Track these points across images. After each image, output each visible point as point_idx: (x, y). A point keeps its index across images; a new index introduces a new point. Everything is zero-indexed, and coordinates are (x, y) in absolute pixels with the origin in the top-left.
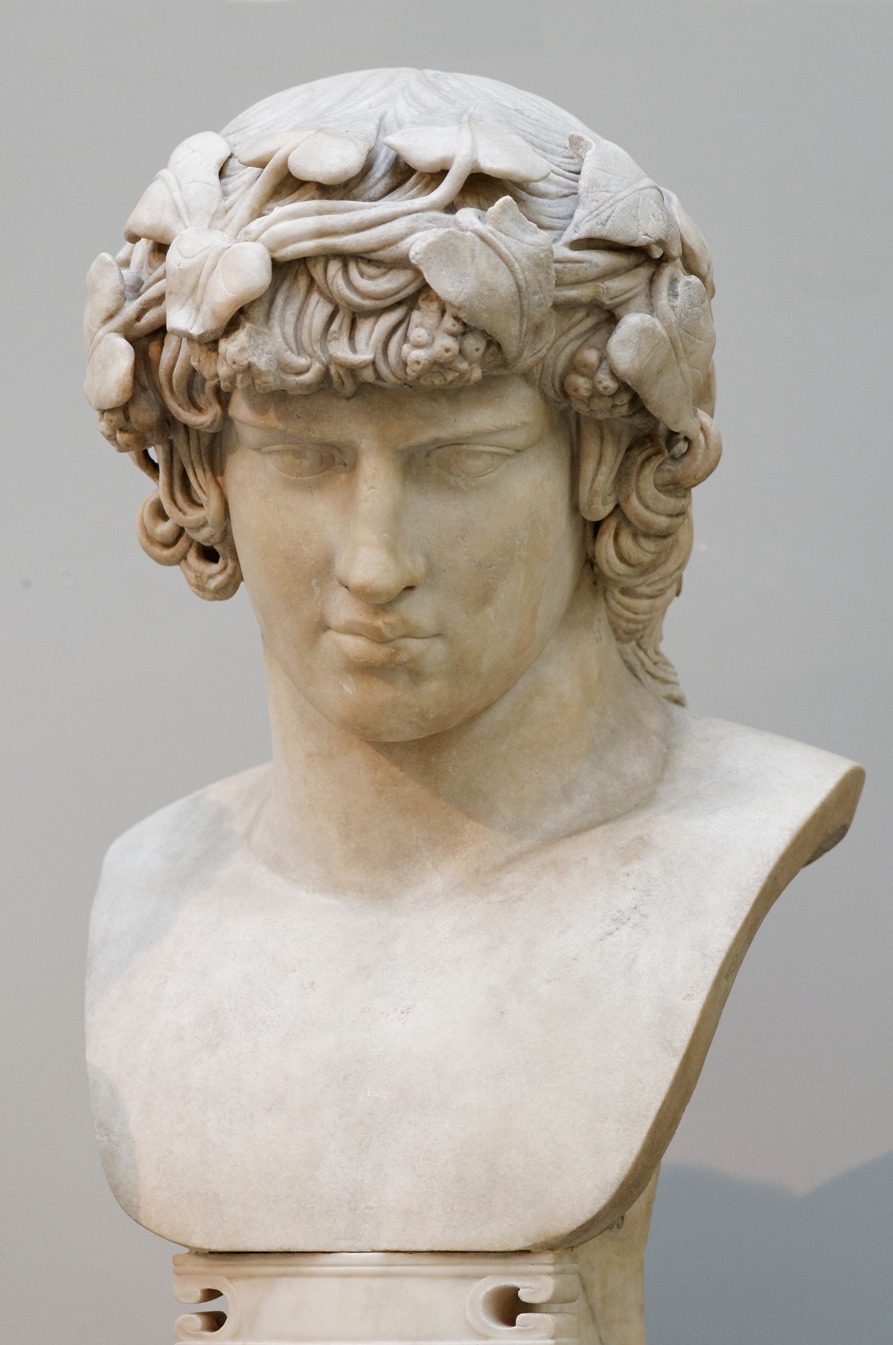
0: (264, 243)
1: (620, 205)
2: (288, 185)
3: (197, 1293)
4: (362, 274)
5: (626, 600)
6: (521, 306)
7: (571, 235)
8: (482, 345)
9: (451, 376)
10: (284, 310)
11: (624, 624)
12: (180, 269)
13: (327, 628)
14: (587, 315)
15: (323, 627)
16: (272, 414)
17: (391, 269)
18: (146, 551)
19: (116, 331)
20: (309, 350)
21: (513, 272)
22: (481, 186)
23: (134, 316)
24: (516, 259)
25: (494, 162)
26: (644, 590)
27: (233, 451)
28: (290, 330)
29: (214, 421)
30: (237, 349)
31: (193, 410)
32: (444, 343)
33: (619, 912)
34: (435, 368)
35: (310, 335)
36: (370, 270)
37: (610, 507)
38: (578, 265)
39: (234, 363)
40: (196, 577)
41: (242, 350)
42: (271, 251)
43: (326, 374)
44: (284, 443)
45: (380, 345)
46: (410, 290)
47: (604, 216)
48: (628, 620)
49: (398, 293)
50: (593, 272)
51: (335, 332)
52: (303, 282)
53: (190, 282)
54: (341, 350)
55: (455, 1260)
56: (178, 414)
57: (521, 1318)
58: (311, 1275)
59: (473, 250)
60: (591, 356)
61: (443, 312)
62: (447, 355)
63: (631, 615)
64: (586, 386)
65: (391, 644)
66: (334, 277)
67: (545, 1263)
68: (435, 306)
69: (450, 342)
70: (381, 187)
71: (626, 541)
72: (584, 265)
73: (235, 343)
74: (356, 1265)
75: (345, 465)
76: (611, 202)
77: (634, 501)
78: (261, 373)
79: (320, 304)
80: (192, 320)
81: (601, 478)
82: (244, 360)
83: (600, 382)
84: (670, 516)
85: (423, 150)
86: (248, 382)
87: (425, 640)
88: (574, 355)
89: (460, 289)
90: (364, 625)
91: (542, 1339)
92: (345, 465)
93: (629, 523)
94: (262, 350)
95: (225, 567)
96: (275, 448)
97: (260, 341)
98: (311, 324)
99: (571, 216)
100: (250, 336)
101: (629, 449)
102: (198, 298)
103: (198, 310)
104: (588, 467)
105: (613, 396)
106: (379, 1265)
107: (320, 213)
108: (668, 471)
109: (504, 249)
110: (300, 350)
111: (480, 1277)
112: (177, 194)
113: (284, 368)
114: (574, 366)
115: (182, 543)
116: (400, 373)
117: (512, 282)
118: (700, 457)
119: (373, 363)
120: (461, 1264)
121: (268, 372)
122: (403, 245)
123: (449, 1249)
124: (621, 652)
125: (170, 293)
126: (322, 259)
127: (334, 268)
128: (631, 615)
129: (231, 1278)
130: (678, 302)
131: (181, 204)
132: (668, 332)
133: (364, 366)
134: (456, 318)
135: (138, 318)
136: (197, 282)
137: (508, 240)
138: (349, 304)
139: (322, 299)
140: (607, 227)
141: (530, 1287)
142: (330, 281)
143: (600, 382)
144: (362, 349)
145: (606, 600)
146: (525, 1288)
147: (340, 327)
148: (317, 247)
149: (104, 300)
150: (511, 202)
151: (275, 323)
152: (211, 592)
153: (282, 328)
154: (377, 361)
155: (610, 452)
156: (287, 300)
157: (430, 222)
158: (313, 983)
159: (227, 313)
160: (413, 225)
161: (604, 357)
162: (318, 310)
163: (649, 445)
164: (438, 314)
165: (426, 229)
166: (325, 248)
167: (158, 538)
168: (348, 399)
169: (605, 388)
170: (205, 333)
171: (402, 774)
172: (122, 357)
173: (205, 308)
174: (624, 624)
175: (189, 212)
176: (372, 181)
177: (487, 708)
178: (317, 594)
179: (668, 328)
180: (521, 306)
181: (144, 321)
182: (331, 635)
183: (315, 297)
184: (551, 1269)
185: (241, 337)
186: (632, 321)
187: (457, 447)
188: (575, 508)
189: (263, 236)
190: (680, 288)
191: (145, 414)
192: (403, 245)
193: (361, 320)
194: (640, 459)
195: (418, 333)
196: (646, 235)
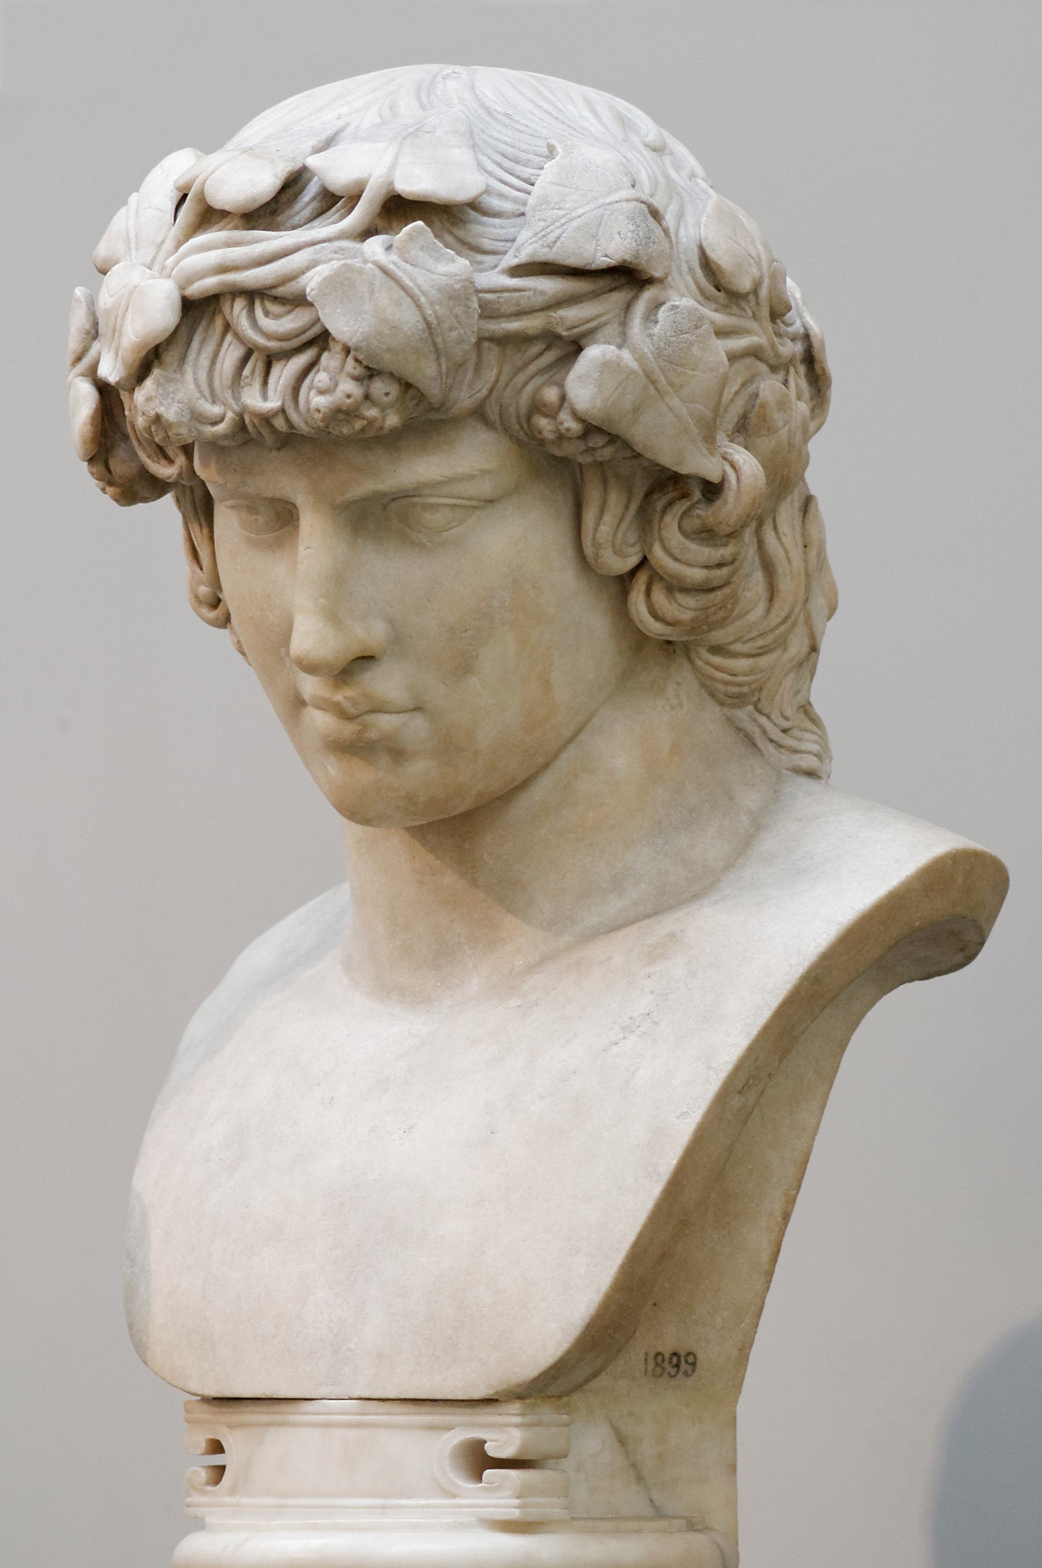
1: (575, 224)
3: (201, 1441)
4: (267, 314)
5: (717, 660)
7: (511, 260)
8: (394, 390)
10: (199, 352)
11: (721, 687)
14: (548, 348)
15: (299, 703)
17: (297, 306)
21: (419, 307)
22: (397, 209)
24: (423, 293)
25: (417, 182)
26: (738, 647)
28: (203, 376)
31: (163, 462)
32: (348, 387)
36: (274, 308)
37: (633, 561)
38: (517, 294)
41: (149, 399)
42: (182, 288)
43: (240, 426)
45: (289, 391)
47: (552, 237)
48: (726, 683)
49: (304, 332)
50: (538, 301)
52: (219, 324)
55: (424, 1409)
58: (296, 1425)
60: (551, 394)
62: (349, 401)
63: (727, 677)
64: (549, 428)
65: (358, 720)
66: (238, 316)
67: (512, 1413)
70: (307, 212)
71: (659, 597)
72: (527, 293)
76: (563, 221)
78: (170, 425)
81: (605, 529)
84: (707, 567)
87: (401, 715)
89: (355, 328)
90: (325, 700)
91: (507, 1498)
93: (662, 578)
94: (173, 398)
97: (171, 389)
99: (514, 240)
100: (158, 384)
101: (649, 494)
104: (589, 517)
106: (355, 1414)
107: (228, 245)
108: (699, 517)
109: (407, 281)
111: (449, 1428)
113: (198, 417)
117: (419, 318)
118: (731, 500)
119: (283, 411)
120: (430, 1414)
121: (179, 424)
122: (303, 280)
124: (730, 721)
126: (229, 297)
127: (240, 304)
128: (727, 677)
129: (231, 1427)
130: (657, 330)
131: (132, 234)
132: (641, 365)
134: (357, 360)
137: (415, 271)
139: (235, 341)
140: (555, 249)
141: (496, 1441)
143: (562, 423)
145: (690, 660)
147: (253, 372)
148: (219, 284)
150: (421, 228)
151: (188, 368)
153: (195, 373)
154: (286, 408)
155: (615, 499)
156: (203, 342)
157: (336, 252)
160: (315, 256)
161: (563, 398)
162: (231, 354)
163: (671, 489)
166: (224, 284)
169: (568, 430)
174: (721, 687)
176: (298, 206)
177: (523, 785)
179: (641, 359)
180: (435, 344)
183: (229, 338)
184: (518, 1420)
185: (149, 383)
187: (408, 499)
188: (584, 563)
190: (662, 313)
194: (659, 506)
195: (321, 377)
196: (606, 256)
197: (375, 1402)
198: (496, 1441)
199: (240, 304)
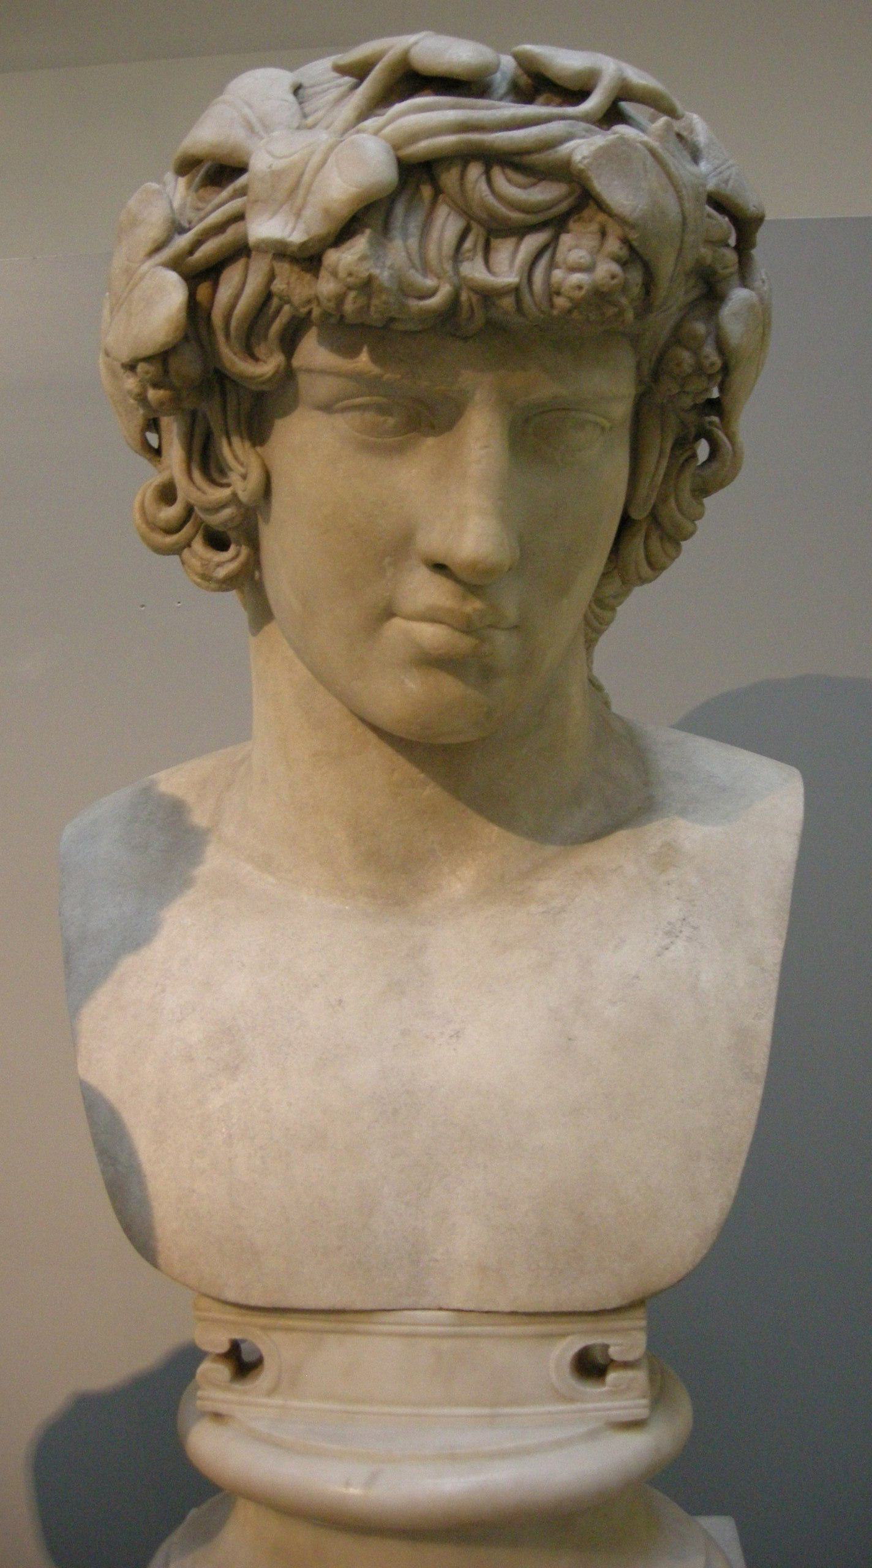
0: (386, 139)
2: (411, 81)
4: (509, 181)
9: (611, 311)
16: (364, 357)
17: (544, 179)
18: (144, 539)
21: (680, 199)
23: (188, 247)
27: (286, 412)
28: (413, 242)
30: (356, 257)
31: (250, 361)
32: (606, 269)
33: (669, 923)
35: (440, 249)
39: (350, 274)
40: (203, 565)
41: (363, 258)
42: (396, 148)
43: (454, 301)
44: (371, 394)
45: (526, 268)
46: (564, 207)
47: (726, 175)
49: (550, 208)
51: (469, 251)
53: (287, 183)
54: (475, 271)
57: (612, 1376)
59: (644, 164)
60: (700, 328)
61: (603, 234)
66: (477, 181)
69: (615, 268)
71: (655, 545)
73: (352, 251)
74: (429, 1325)
75: (433, 427)
77: (672, 503)
78: (382, 289)
79: (451, 218)
80: (290, 226)
82: (365, 270)
83: (707, 357)
85: (566, 60)
86: (362, 301)
88: (678, 327)
94: (384, 263)
95: (237, 555)
102: (299, 201)
103: (298, 215)
105: (710, 377)
106: (454, 1325)
112: (246, 110)
113: (405, 290)
114: (677, 337)
115: (188, 529)
116: (545, 306)
119: (516, 290)
125: (256, 201)
127: (475, 171)
131: (254, 120)
134: (625, 241)
135: (191, 252)
136: (298, 183)
138: (493, 216)
144: (505, 266)
147: (475, 245)
149: (153, 227)
151: (396, 233)
152: (218, 581)
158: (340, 1001)
159: (346, 213)
160: (570, 130)
162: (447, 226)
164: (598, 236)
165: (583, 137)
166: (469, 143)
167: (162, 524)
168: (465, 339)
169: (712, 364)
171: (422, 776)
172: (170, 295)
173: (308, 213)
178: (389, 574)
180: (682, 242)
181: (199, 254)
182: (397, 622)
183: (442, 211)
185: (360, 244)
186: (739, 296)
189: (387, 130)
191: (188, 366)
193: (499, 241)
199: (475, 171)
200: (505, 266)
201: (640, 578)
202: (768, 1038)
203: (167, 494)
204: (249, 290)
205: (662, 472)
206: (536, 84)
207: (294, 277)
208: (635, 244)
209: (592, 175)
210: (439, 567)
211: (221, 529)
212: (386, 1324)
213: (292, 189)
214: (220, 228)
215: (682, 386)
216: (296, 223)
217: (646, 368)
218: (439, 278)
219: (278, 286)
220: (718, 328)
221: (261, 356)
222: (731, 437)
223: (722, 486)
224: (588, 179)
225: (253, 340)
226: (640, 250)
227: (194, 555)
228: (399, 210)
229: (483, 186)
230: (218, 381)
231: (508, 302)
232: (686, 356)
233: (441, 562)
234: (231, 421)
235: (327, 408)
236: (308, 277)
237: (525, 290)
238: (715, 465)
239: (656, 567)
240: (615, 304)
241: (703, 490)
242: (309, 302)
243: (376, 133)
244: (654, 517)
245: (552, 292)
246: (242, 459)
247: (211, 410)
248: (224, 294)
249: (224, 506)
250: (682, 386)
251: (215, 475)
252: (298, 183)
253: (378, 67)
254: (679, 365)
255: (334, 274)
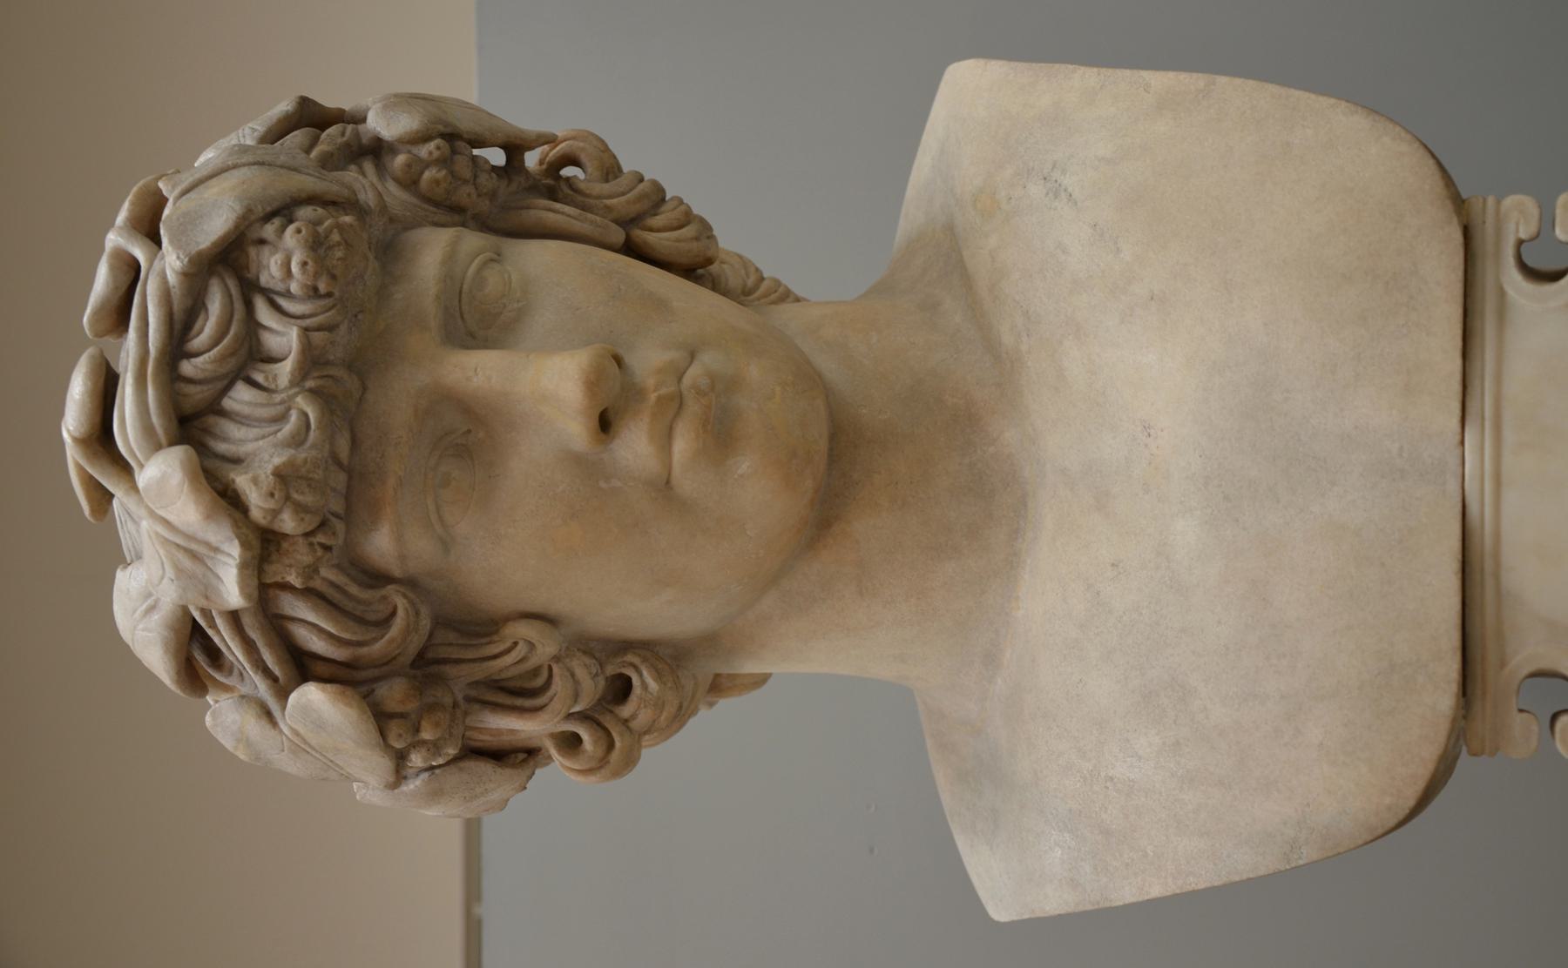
2: (101, 438)
5: (756, 295)
6: (282, 167)
9: (336, 237)
12: (178, 578)
13: (668, 482)
18: (617, 774)
19: (284, 708)
20: (280, 409)
21: (235, 167)
28: (254, 432)
29: (405, 596)
32: (290, 238)
34: (321, 251)
35: (262, 405)
41: (255, 481)
42: (158, 447)
43: (315, 393)
46: (232, 284)
49: (230, 296)
51: (267, 379)
52: (212, 420)
53: (187, 562)
56: (392, 641)
61: (262, 242)
68: (252, 251)
69: (291, 228)
78: (291, 463)
82: (267, 478)
92: (469, 431)
96: (432, 507)
98: (249, 404)
103: (216, 550)
105: (454, 152)
110: (281, 418)
111: (1502, 293)
113: (297, 440)
114: (410, 183)
117: (244, 170)
119: (306, 330)
123: (1460, 273)
127: (187, 368)
129: (1503, 664)
133: (307, 347)
135: (275, 680)
136: (187, 551)
141: (1517, 224)
142: (200, 375)
144: (284, 338)
146: (1517, 231)
151: (242, 450)
156: (225, 439)
166: (157, 374)
167: (600, 752)
168: (365, 389)
169: (438, 148)
170: (238, 537)
175: (150, 595)
178: (619, 484)
181: (277, 671)
183: (227, 403)
191: (393, 693)
192: (172, 278)
197: (1468, 398)
198: (1517, 224)
200: (284, 338)
201: (697, 239)
202: (1171, 74)
203: (570, 743)
204: (311, 617)
205: (567, 209)
206: (119, 312)
207: (287, 562)
208: (269, 209)
209: (194, 249)
210: (605, 424)
211: (602, 682)
212: (1483, 513)
213: (192, 556)
214: (249, 646)
215: (466, 182)
216: (223, 552)
217: (443, 218)
218: (289, 409)
219: (293, 579)
220: (401, 141)
221: (387, 612)
222: (551, 140)
223: (606, 149)
224: (200, 254)
225: (372, 617)
226: (276, 205)
227: (634, 716)
228: (222, 447)
229: (199, 361)
230: (425, 667)
231: (317, 337)
232: (427, 175)
233: (596, 422)
234: (470, 654)
235: (446, 543)
236: (285, 545)
237: (308, 322)
238: (584, 158)
239: (688, 218)
240: (329, 232)
241: (611, 169)
242: (311, 544)
243: (142, 466)
244: (627, 223)
245: (313, 293)
246: (508, 644)
247: (461, 677)
248: (317, 645)
249: (573, 675)
250: (466, 182)
251: (540, 681)
252: (187, 551)
253: (90, 471)
254: (437, 182)
255: (275, 513)
